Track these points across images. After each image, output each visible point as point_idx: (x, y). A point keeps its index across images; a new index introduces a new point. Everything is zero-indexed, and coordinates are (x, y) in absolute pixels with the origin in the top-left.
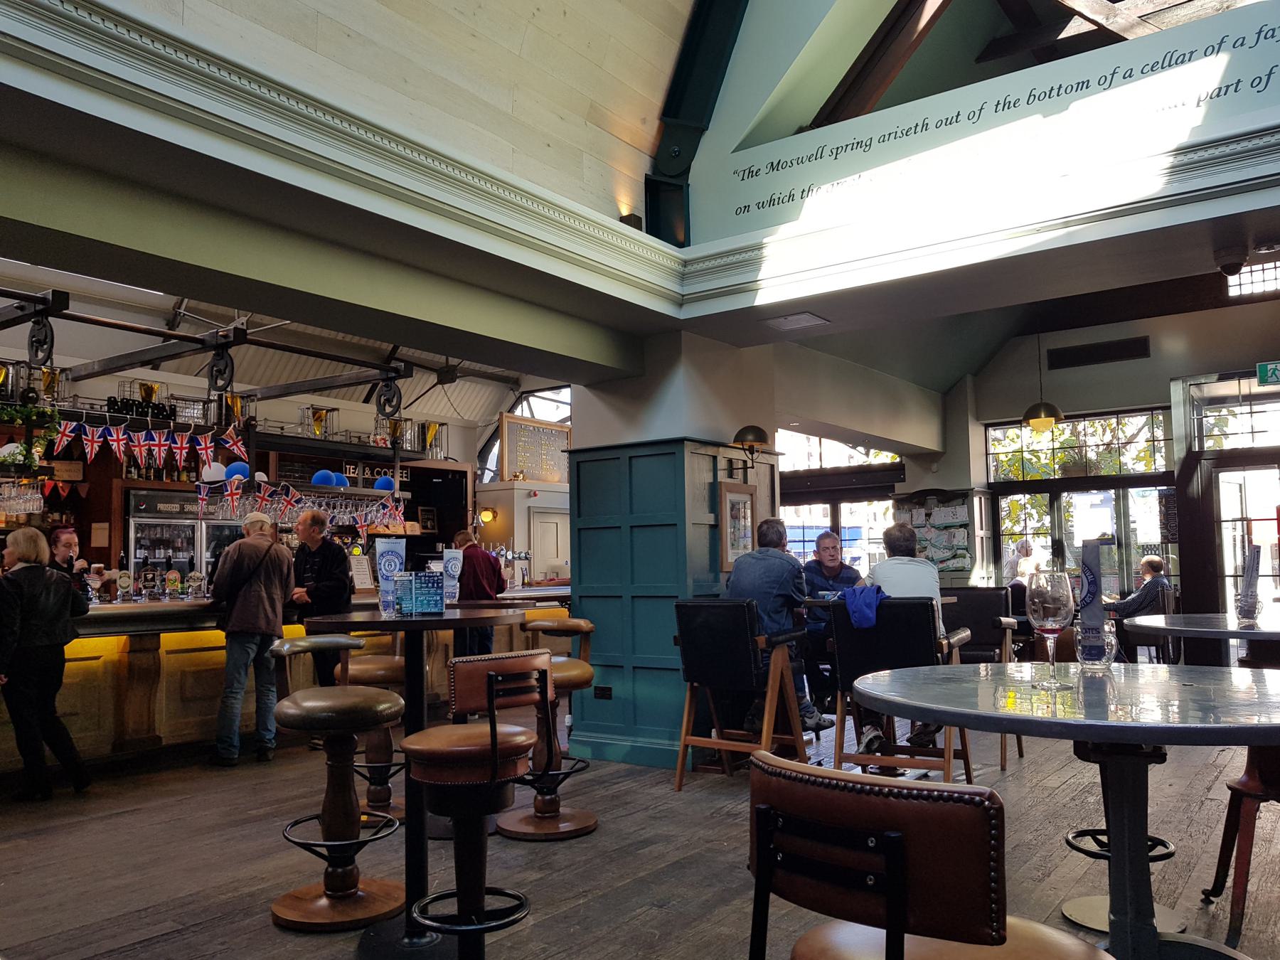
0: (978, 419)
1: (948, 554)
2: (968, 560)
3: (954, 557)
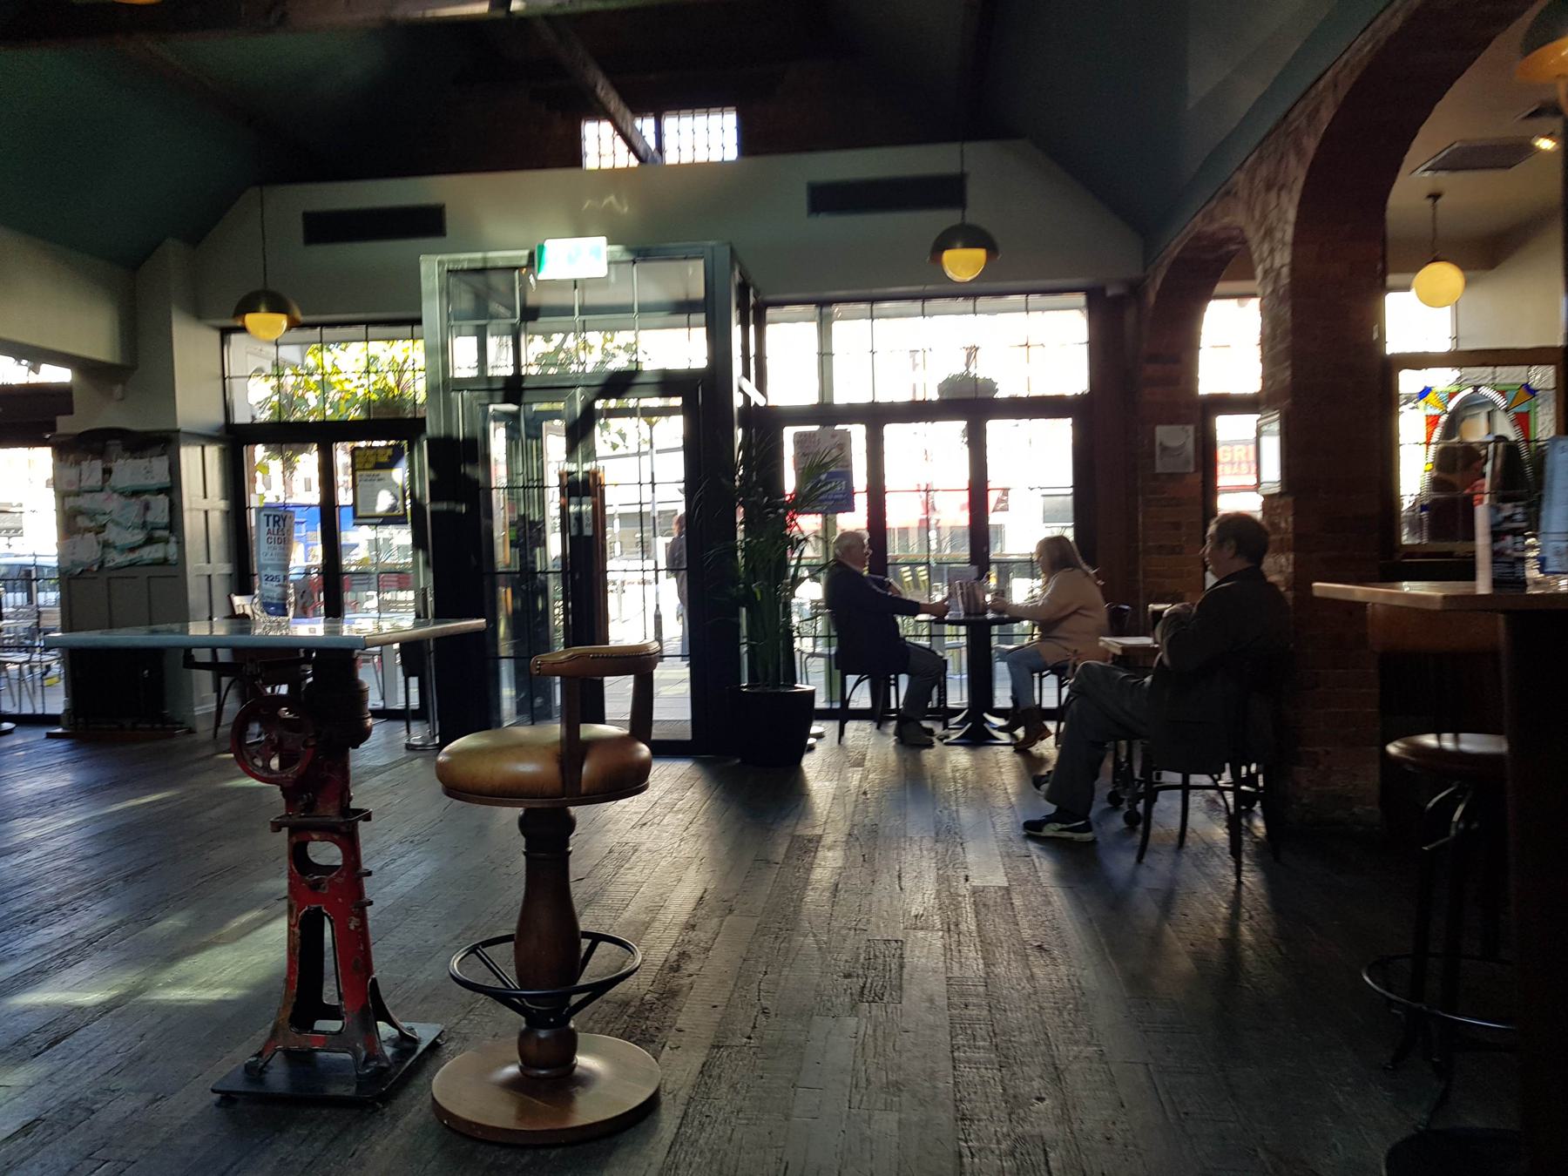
0: (198, 313)
1: (139, 537)
2: (172, 549)
3: (150, 541)
